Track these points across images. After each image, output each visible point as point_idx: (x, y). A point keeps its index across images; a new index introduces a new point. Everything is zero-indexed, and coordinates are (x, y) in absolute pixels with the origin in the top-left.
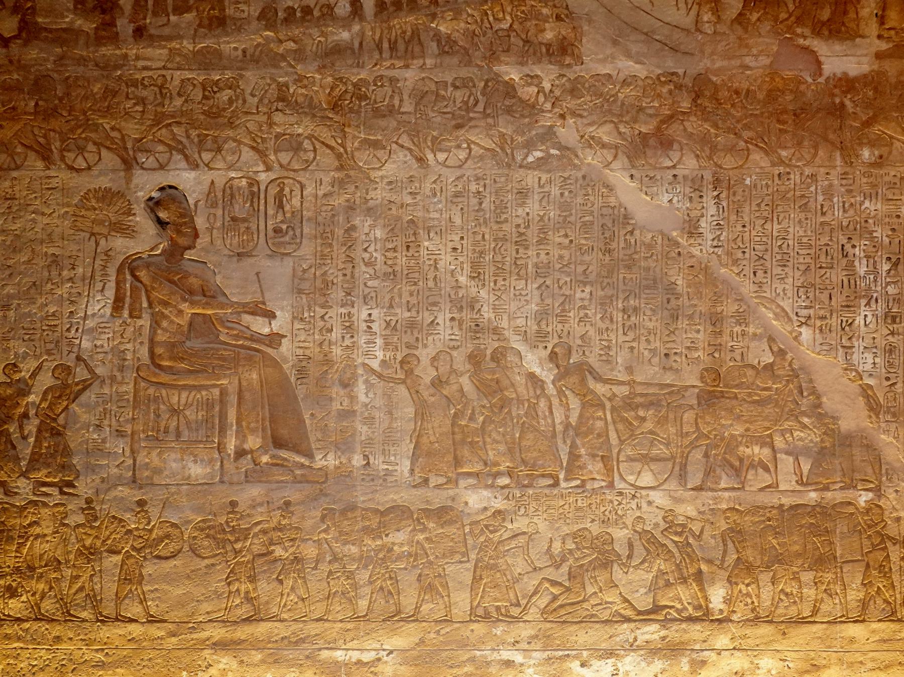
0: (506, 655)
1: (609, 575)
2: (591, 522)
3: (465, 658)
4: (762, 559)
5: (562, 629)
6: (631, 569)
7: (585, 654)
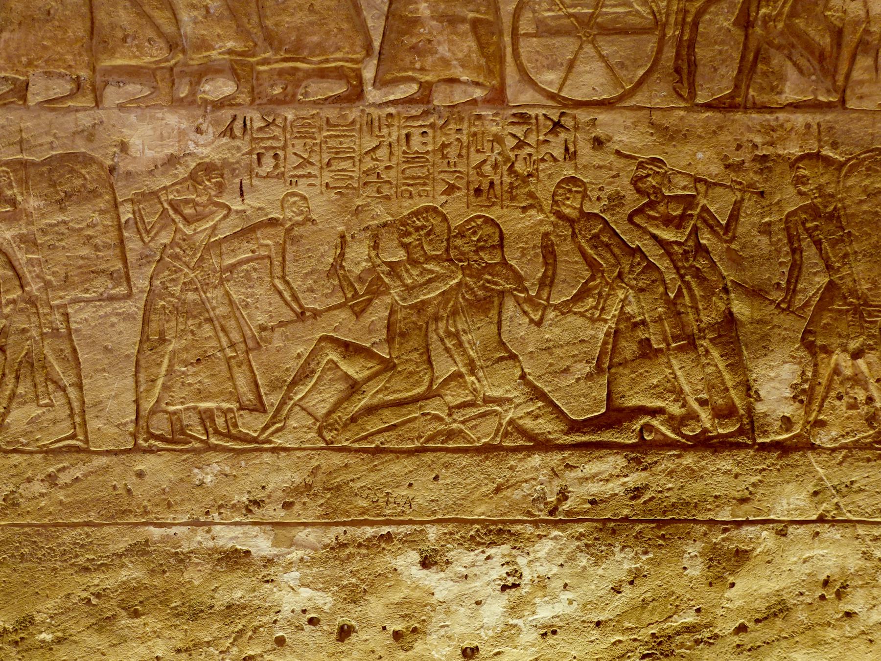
0: (227, 537)
1: (494, 328)
2: (447, 192)
3: (121, 547)
5: (374, 469)
6: (551, 315)
7: (433, 533)
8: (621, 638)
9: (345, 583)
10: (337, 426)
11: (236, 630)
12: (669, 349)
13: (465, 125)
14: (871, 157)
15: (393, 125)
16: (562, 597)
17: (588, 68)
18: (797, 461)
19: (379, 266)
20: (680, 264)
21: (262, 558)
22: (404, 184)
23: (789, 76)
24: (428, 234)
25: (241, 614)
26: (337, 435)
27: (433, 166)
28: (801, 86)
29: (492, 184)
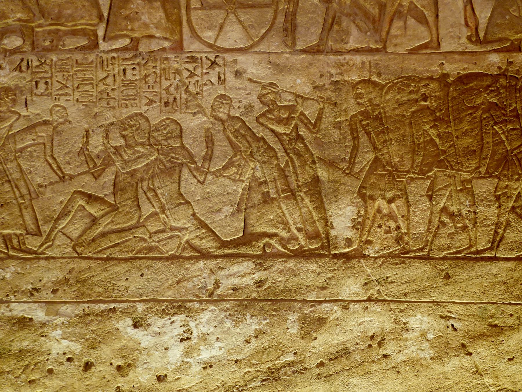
0: (19, 310)
1: (176, 186)
2: (147, 104)
4: (414, 161)
5: (105, 270)
6: (210, 177)
7: (140, 307)
8: (250, 370)
9: (88, 337)
10: (84, 244)
11: (25, 364)
12: (280, 198)
13: (158, 63)
14: (401, 81)
15: (115, 64)
16: (216, 345)
17: (231, 29)
18: (354, 264)
19: (109, 148)
20: (287, 147)
21: (40, 322)
22: (123, 99)
23: (352, 32)
24: (137, 129)
25: (27, 355)
26: (84, 249)
27: (140, 88)
28: (360, 38)
29: (175, 99)
